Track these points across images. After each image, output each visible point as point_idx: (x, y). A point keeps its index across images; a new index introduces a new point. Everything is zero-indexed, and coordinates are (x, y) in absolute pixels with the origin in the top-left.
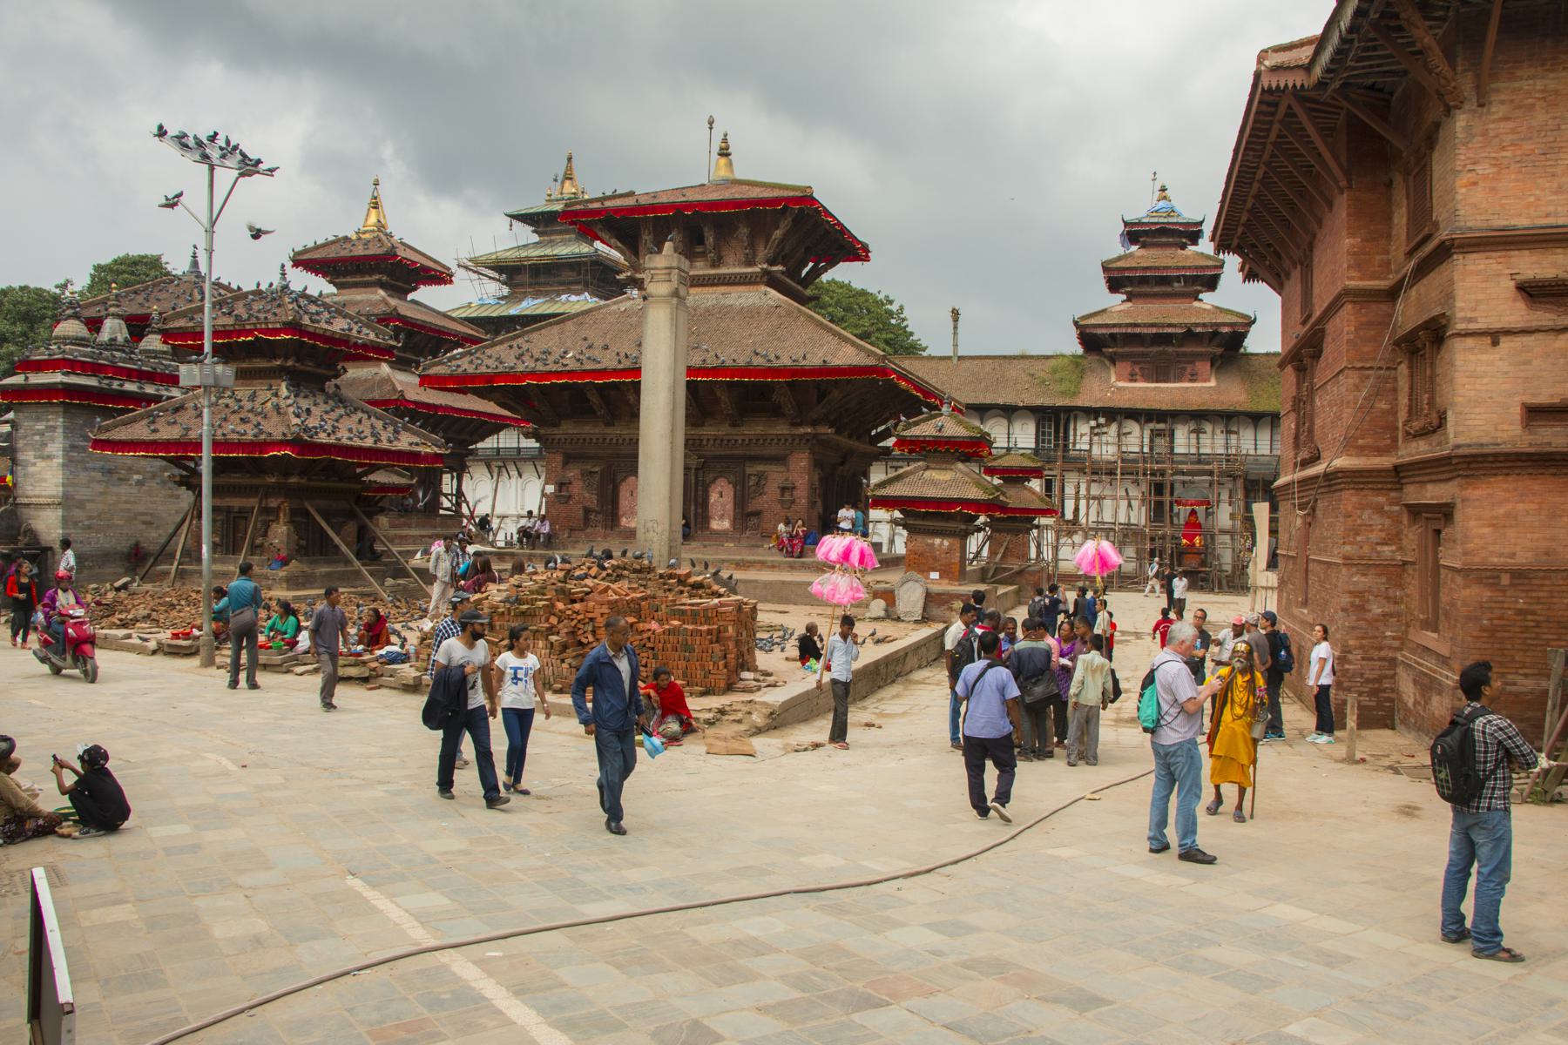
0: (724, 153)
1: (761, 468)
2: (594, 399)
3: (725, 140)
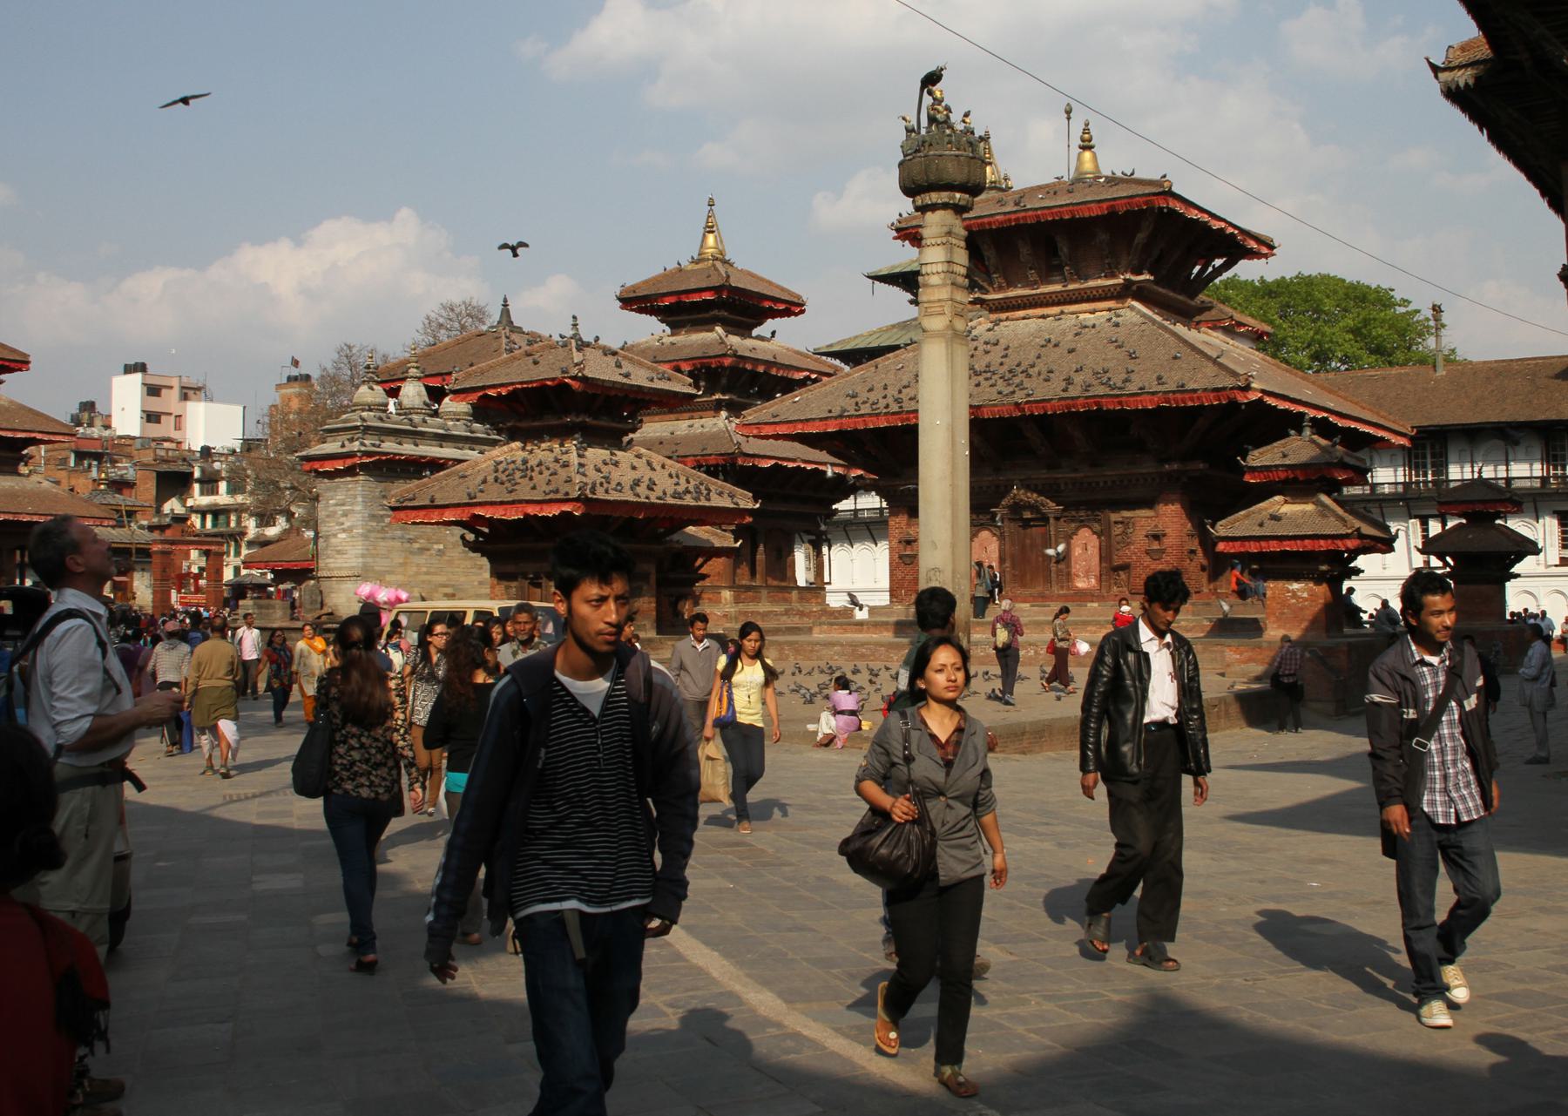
0: (1086, 146)
1: (1126, 514)
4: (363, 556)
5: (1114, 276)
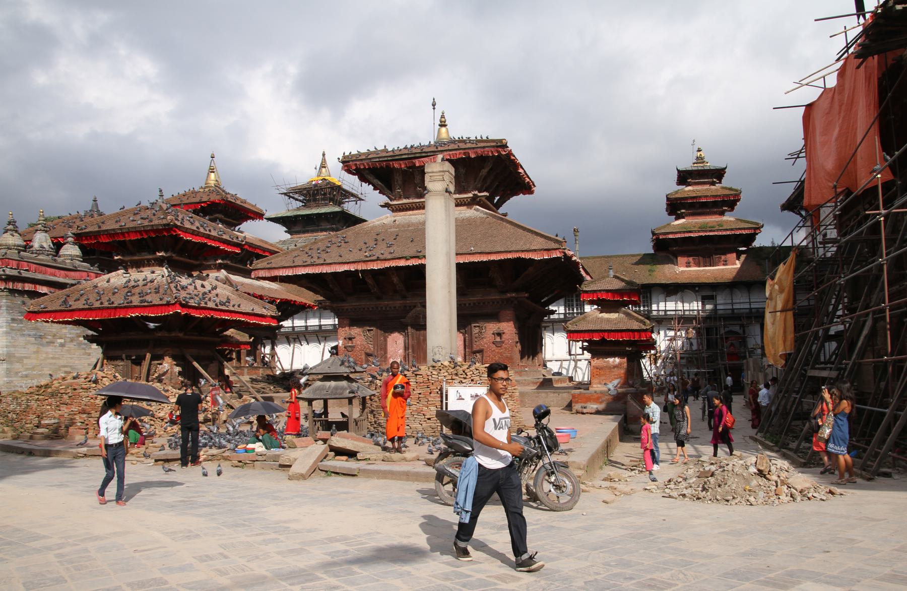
0: (443, 125)
3: (443, 117)
4: (7, 346)
5: (466, 193)
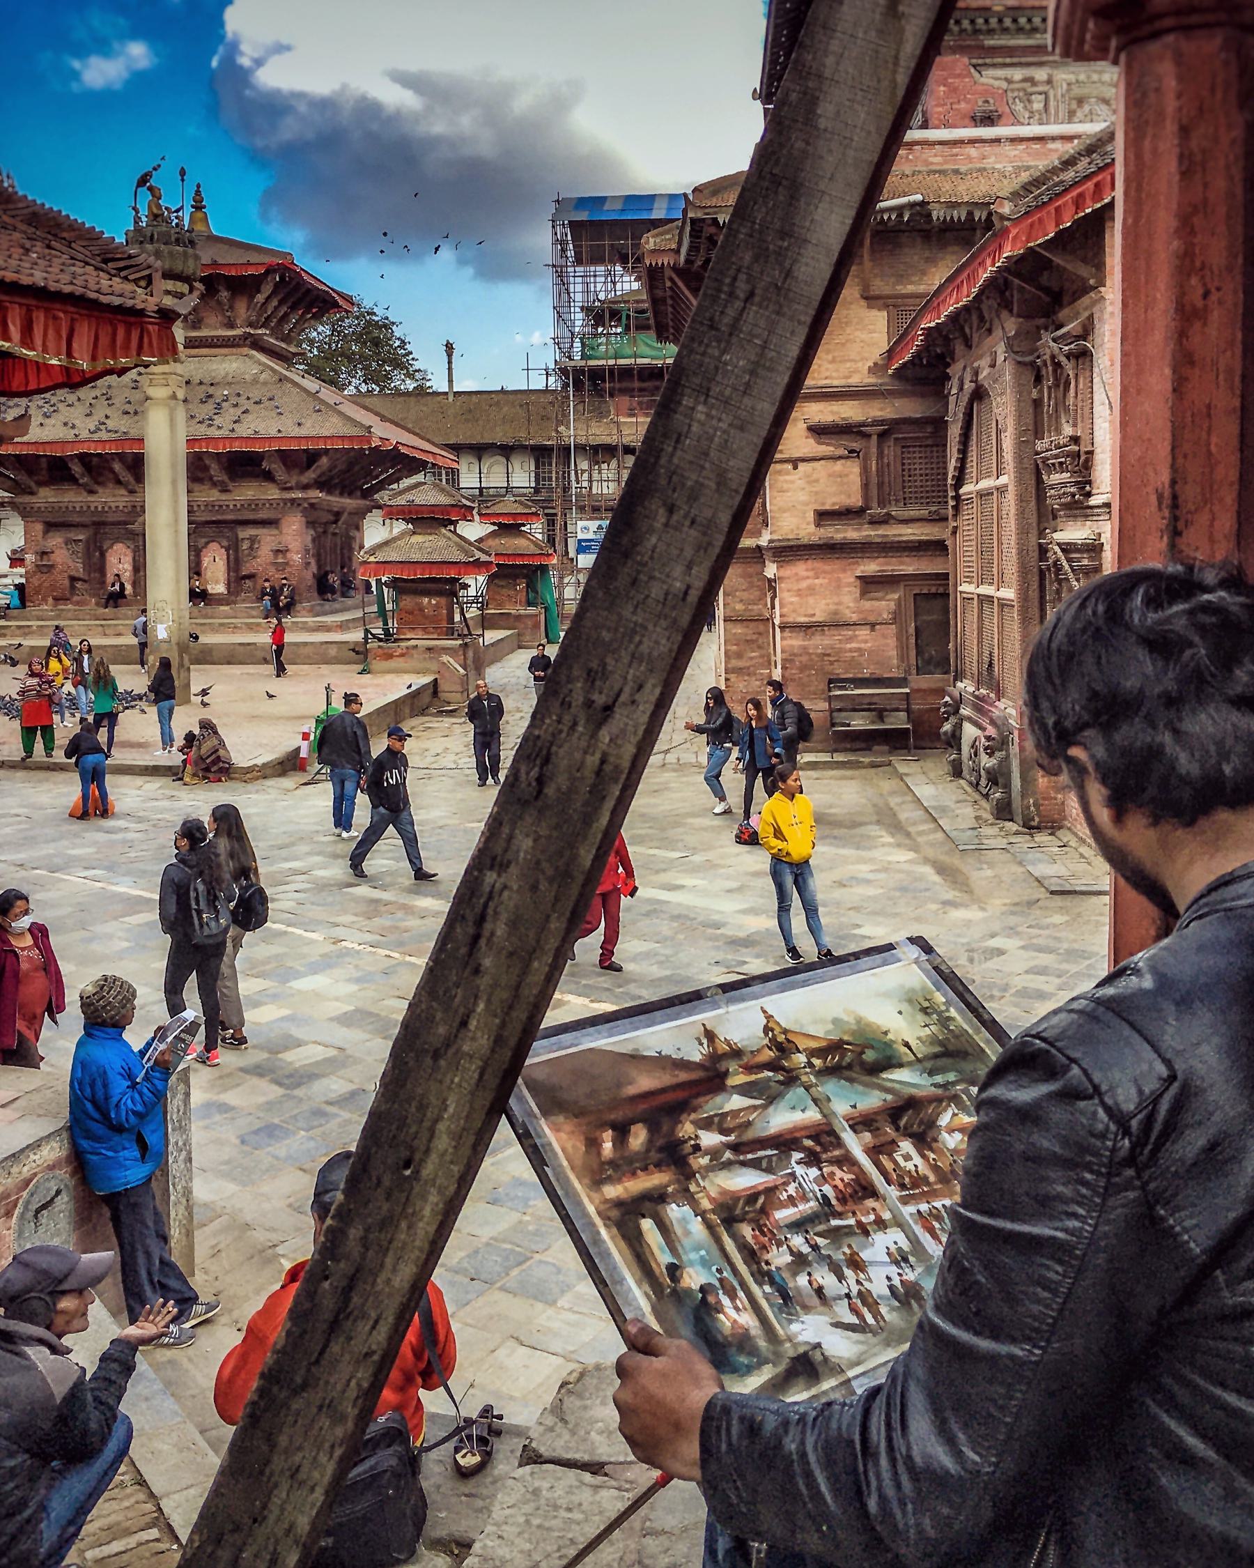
2: (76, 469)
3: (198, 192)
